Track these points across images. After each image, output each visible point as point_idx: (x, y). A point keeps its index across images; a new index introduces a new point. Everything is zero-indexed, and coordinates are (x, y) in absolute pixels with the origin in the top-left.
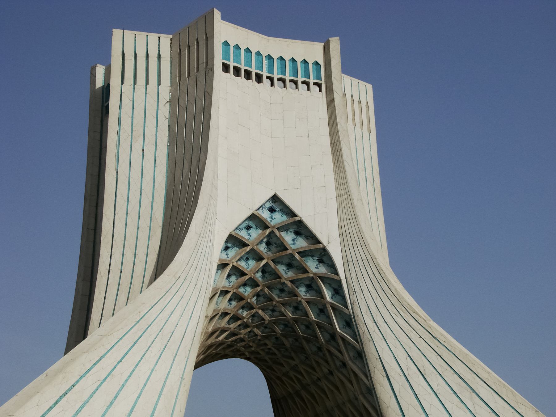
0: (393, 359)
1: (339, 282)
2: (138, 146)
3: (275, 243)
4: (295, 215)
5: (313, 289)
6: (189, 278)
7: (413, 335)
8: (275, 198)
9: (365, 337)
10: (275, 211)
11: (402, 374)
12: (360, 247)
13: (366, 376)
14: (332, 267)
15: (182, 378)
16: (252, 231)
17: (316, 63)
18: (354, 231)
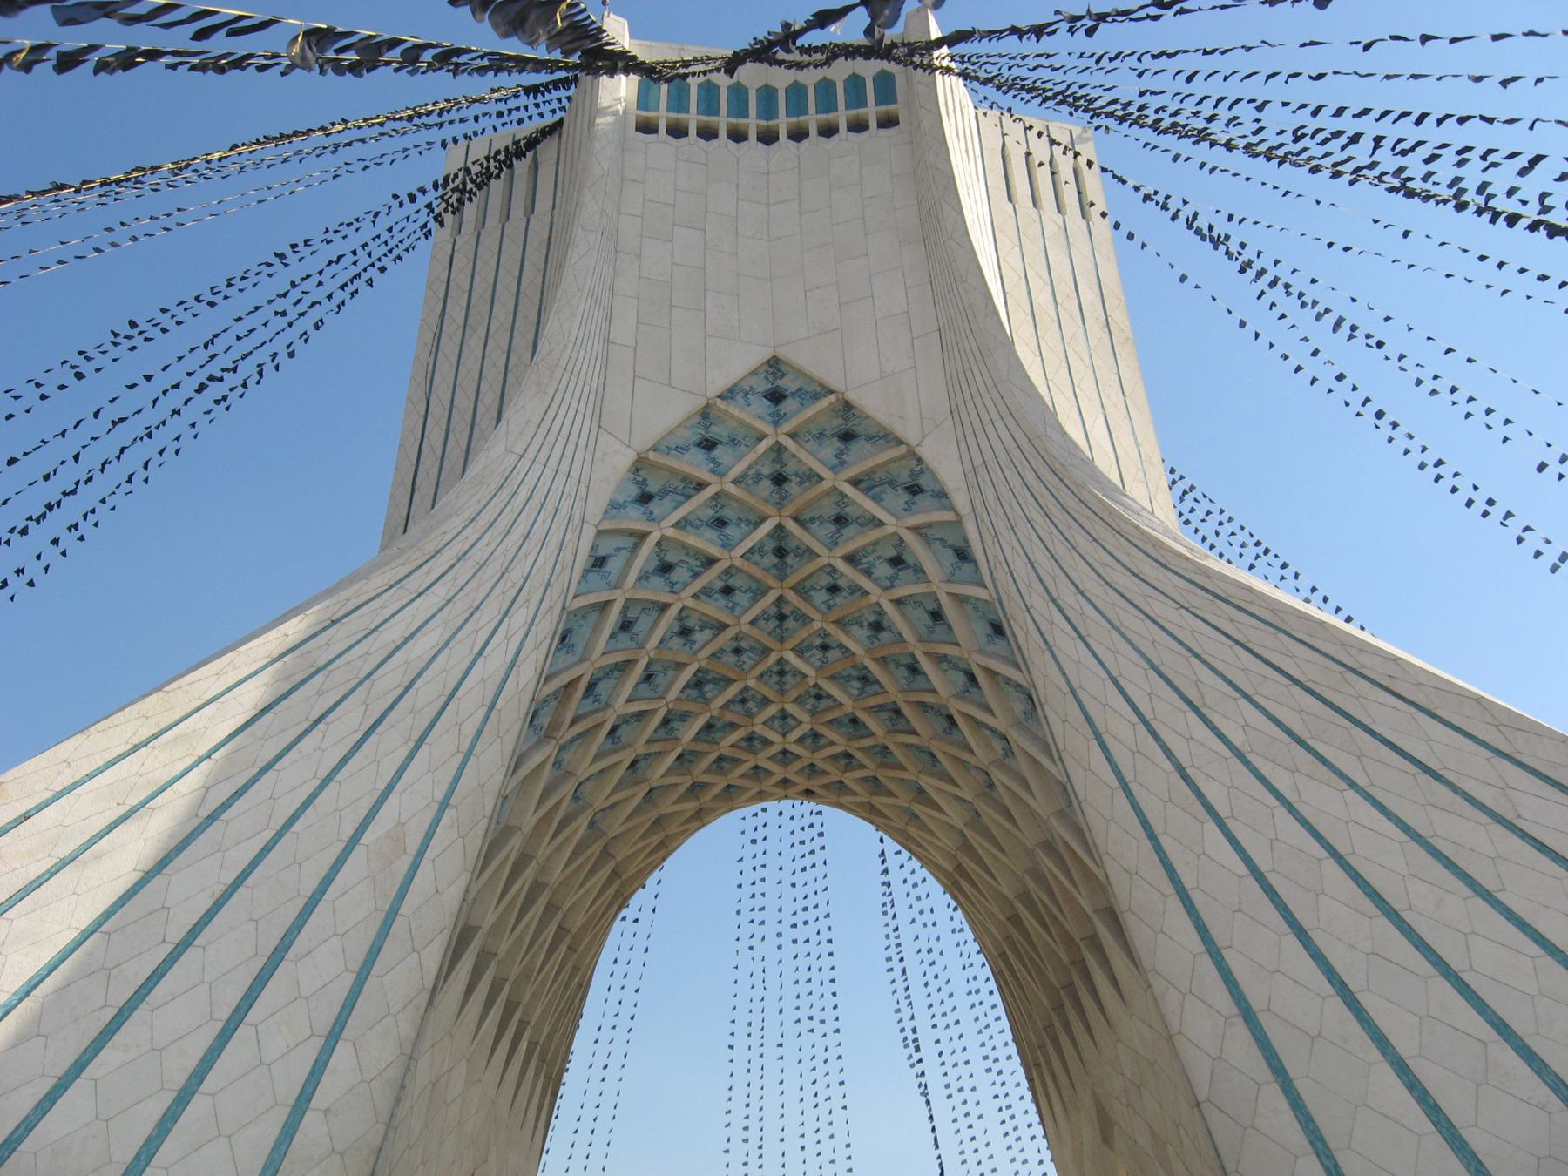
0: (1109, 684)
1: (958, 522)
2: (474, 343)
3: (796, 474)
4: (831, 392)
5: (908, 567)
6: (478, 555)
7: (1160, 608)
10: (785, 397)
11: (1135, 719)
12: (999, 424)
13: (1046, 749)
14: (941, 495)
15: (444, 804)
16: (717, 452)
18: (982, 388)
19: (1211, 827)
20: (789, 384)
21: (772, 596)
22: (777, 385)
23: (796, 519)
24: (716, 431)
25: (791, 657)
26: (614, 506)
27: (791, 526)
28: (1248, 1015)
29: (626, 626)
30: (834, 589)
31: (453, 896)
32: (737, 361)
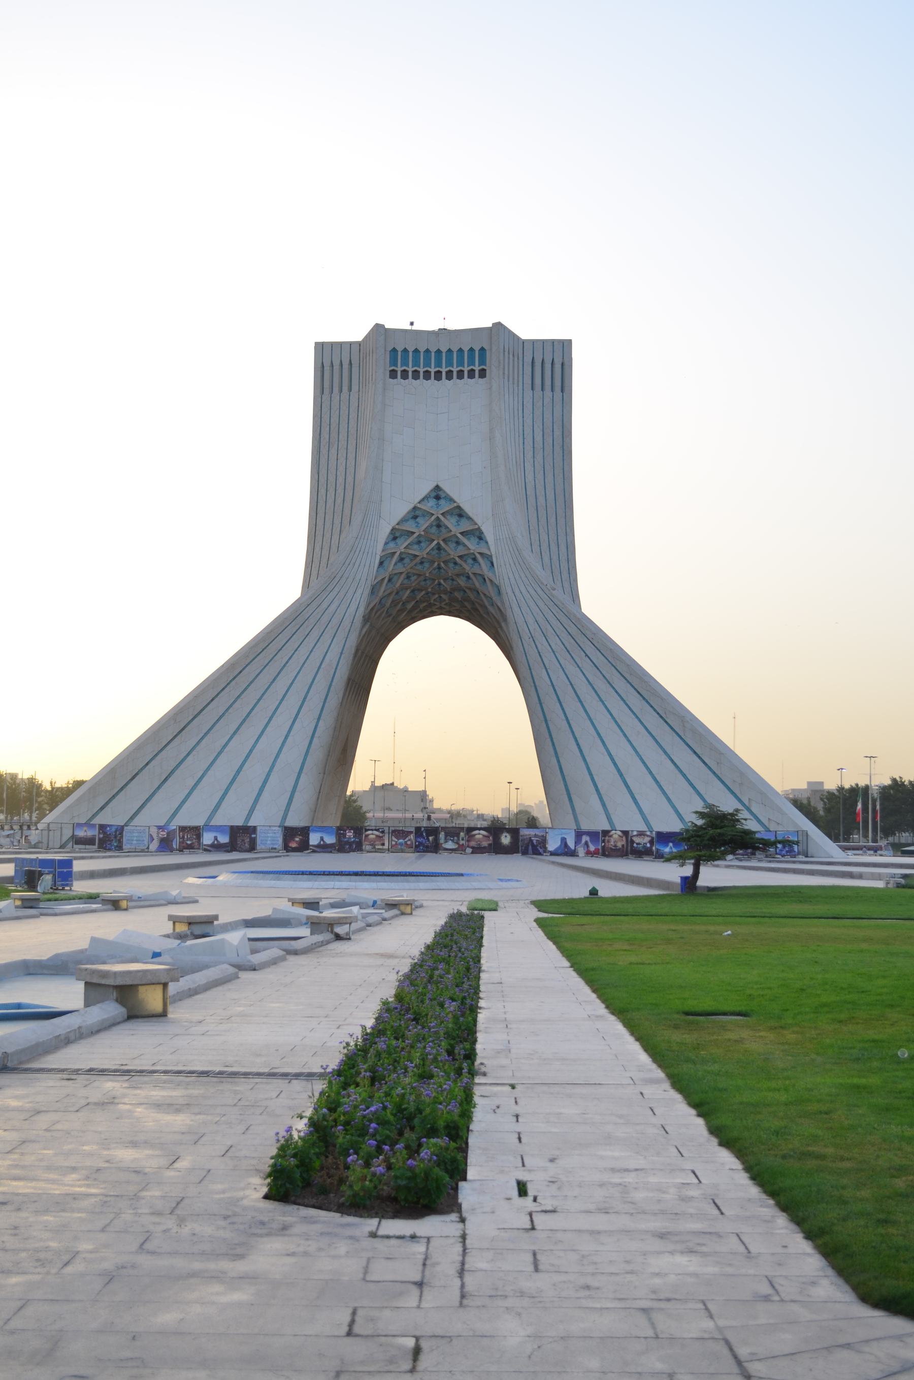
1: (491, 556)
6: (346, 575)
8: (437, 488)
9: (507, 604)
14: (487, 542)
15: (341, 653)
16: (418, 520)
17: (482, 350)
19: (544, 670)
20: (443, 495)
21: (436, 564)
22: (437, 494)
23: (444, 540)
24: (418, 513)
25: (442, 581)
26: (386, 543)
27: (442, 543)
28: (546, 721)
29: (390, 580)
30: (455, 563)
31: (345, 677)
32: (426, 488)
